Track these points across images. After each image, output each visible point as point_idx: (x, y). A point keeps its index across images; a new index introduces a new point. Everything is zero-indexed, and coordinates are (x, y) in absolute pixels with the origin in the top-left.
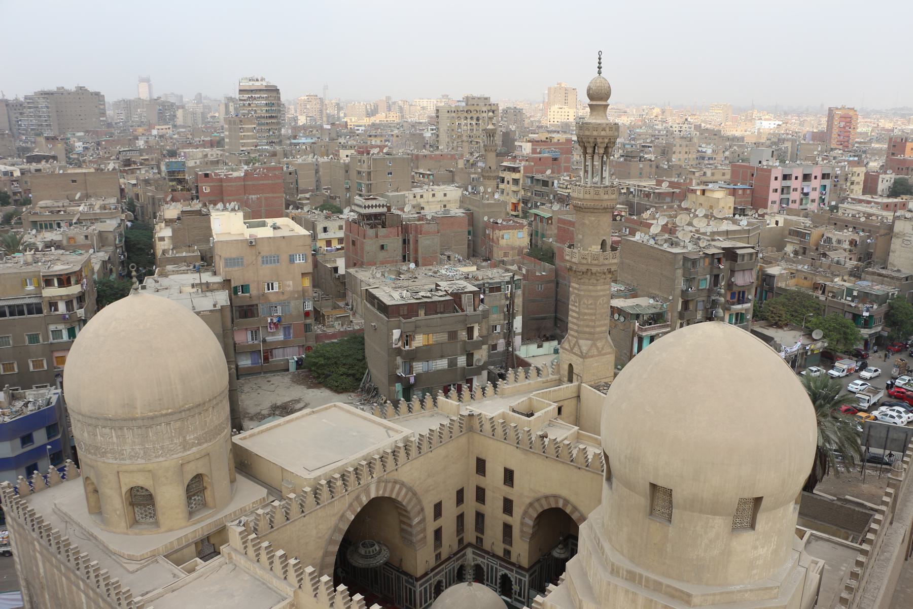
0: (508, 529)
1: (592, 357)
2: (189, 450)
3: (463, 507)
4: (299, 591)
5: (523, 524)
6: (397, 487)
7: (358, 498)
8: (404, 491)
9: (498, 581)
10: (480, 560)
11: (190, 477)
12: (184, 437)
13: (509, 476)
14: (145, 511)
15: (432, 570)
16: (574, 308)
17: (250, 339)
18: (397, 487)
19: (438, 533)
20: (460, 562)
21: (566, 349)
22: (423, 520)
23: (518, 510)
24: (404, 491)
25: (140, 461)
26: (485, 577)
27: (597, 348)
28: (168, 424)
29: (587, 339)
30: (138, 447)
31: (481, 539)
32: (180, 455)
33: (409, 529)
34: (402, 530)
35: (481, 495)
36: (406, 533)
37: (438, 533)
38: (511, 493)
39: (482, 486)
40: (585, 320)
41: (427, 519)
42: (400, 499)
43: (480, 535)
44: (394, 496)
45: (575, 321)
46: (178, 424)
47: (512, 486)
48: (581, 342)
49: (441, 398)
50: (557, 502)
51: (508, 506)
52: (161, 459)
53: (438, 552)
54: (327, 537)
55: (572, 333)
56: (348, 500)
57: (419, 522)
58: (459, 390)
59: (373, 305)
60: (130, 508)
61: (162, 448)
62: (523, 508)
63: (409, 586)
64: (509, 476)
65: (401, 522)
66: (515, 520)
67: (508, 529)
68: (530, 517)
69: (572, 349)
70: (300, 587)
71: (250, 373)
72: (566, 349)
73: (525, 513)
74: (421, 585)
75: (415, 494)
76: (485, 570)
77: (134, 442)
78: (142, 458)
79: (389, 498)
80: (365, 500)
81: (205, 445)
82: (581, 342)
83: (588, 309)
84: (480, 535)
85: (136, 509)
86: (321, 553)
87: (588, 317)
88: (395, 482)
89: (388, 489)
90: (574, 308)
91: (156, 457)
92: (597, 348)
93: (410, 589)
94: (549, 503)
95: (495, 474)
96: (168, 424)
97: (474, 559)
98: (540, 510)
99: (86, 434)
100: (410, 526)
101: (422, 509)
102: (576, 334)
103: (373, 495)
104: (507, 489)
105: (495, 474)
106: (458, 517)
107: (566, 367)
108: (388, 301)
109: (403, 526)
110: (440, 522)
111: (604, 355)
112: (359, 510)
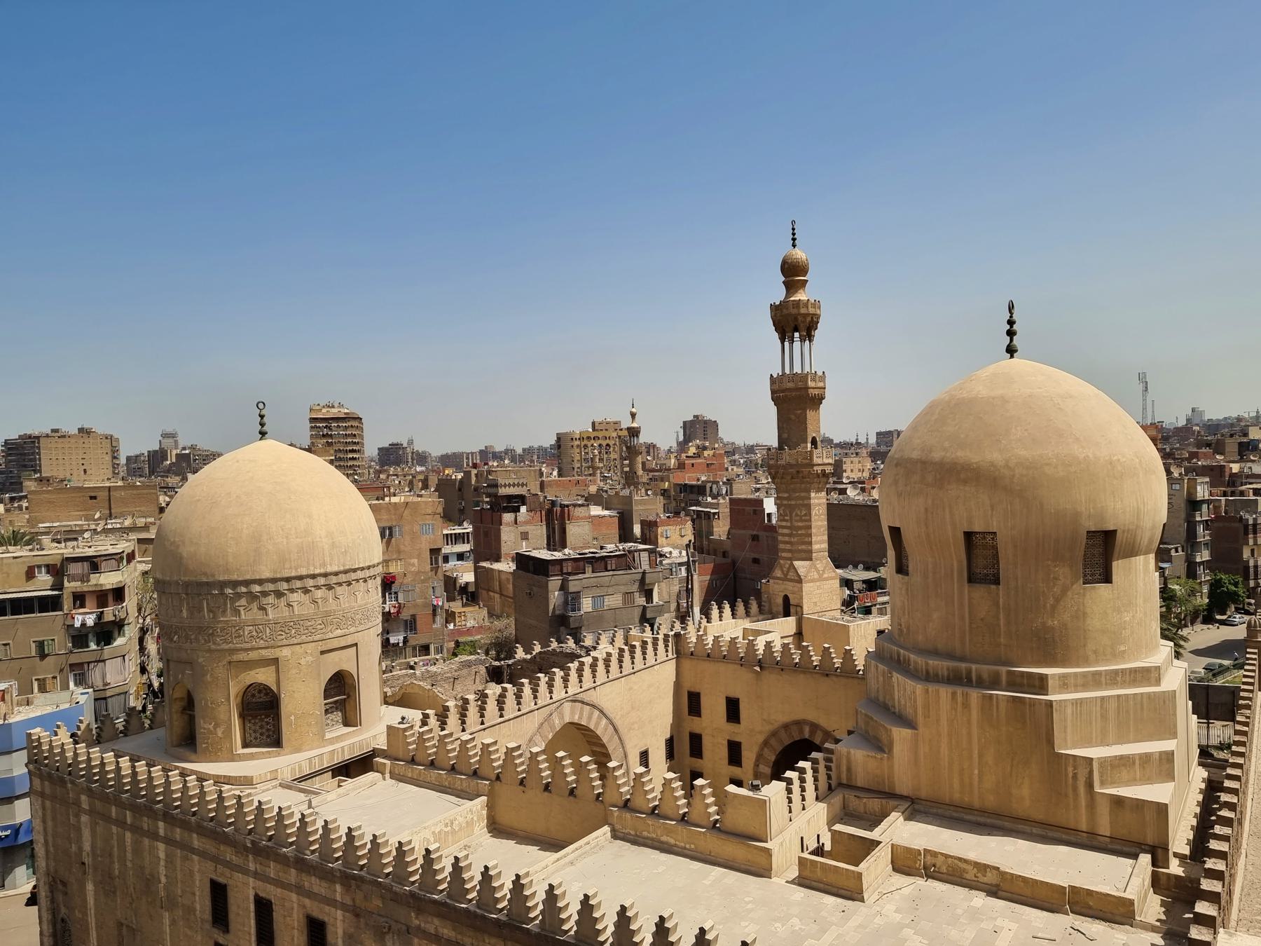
1: (813, 581)
13: (733, 710)
27: (818, 571)
38: (739, 732)
39: (697, 731)
40: (801, 535)
45: (787, 539)
47: (738, 722)
48: (796, 563)
50: (801, 731)
55: (784, 555)
56: (537, 717)
62: (756, 749)
64: (733, 710)
69: (786, 575)
73: (759, 758)
82: (796, 563)
92: (818, 571)
95: (713, 708)
102: (789, 555)
103: (567, 720)
104: (732, 727)
105: (713, 708)
107: (780, 601)
111: (827, 579)
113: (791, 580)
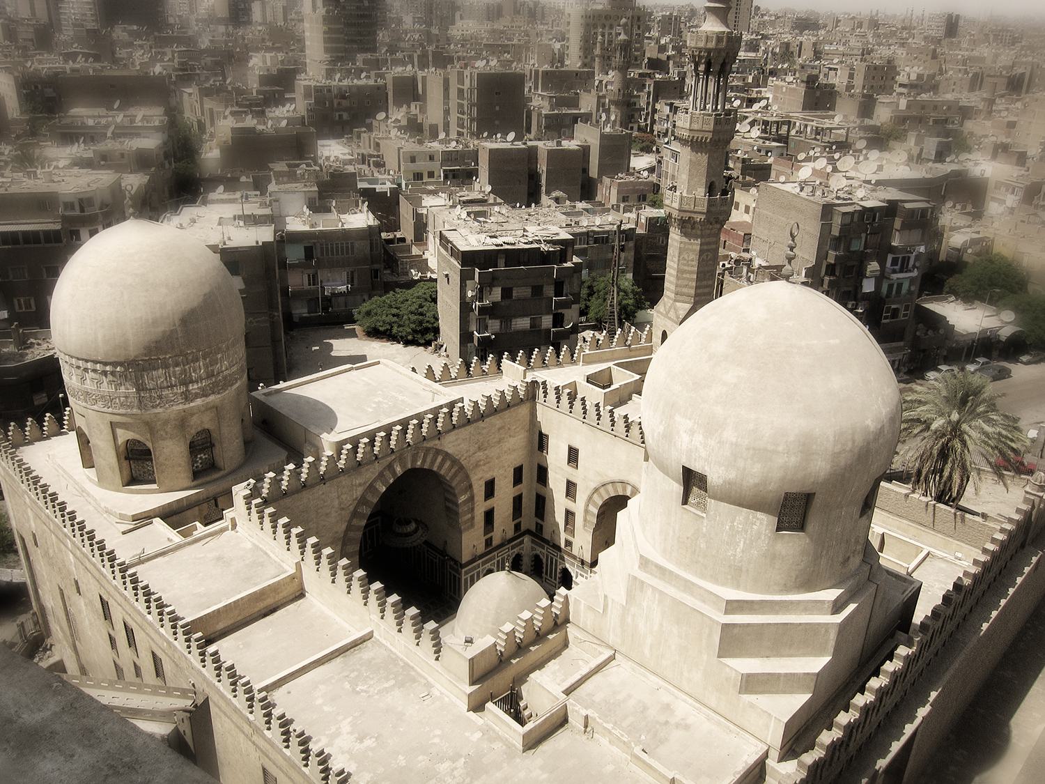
0: (569, 514)
3: (523, 488)
4: (302, 563)
5: (586, 511)
6: (439, 459)
7: (390, 467)
8: (448, 464)
9: (558, 575)
10: (539, 550)
13: (573, 455)
15: (481, 556)
16: (672, 264)
17: (306, 282)
18: (439, 459)
19: (489, 515)
20: (516, 550)
21: (661, 314)
22: (472, 498)
23: (582, 496)
24: (448, 464)
26: (544, 570)
29: (683, 302)
31: (542, 526)
32: (181, 407)
33: (454, 507)
34: (448, 509)
35: (542, 474)
36: (451, 512)
37: (489, 515)
38: (577, 476)
41: (476, 499)
42: (442, 472)
43: (540, 521)
44: (435, 469)
48: (678, 304)
49: (506, 363)
51: (571, 488)
53: (489, 536)
54: (352, 508)
57: (465, 502)
58: (529, 356)
59: (446, 249)
60: (125, 464)
61: (160, 397)
62: (588, 492)
63: (453, 572)
64: (573, 455)
65: (446, 499)
66: (578, 507)
67: (569, 514)
68: (595, 504)
70: (303, 560)
71: (306, 324)
72: (661, 314)
74: (466, 573)
75: (462, 468)
76: (544, 561)
79: (430, 471)
80: (399, 470)
81: (212, 398)
83: (688, 265)
84: (540, 521)
86: (344, 526)
87: (688, 276)
88: (438, 452)
89: (429, 460)
90: (672, 264)
91: (153, 407)
93: (455, 576)
94: (616, 490)
97: (533, 549)
98: (606, 497)
99: (74, 377)
100: (457, 505)
101: (470, 486)
103: (409, 466)
104: (569, 469)
106: (514, 498)
108: (463, 247)
109: (447, 504)
110: (490, 503)
112: (391, 481)
113: (670, 318)
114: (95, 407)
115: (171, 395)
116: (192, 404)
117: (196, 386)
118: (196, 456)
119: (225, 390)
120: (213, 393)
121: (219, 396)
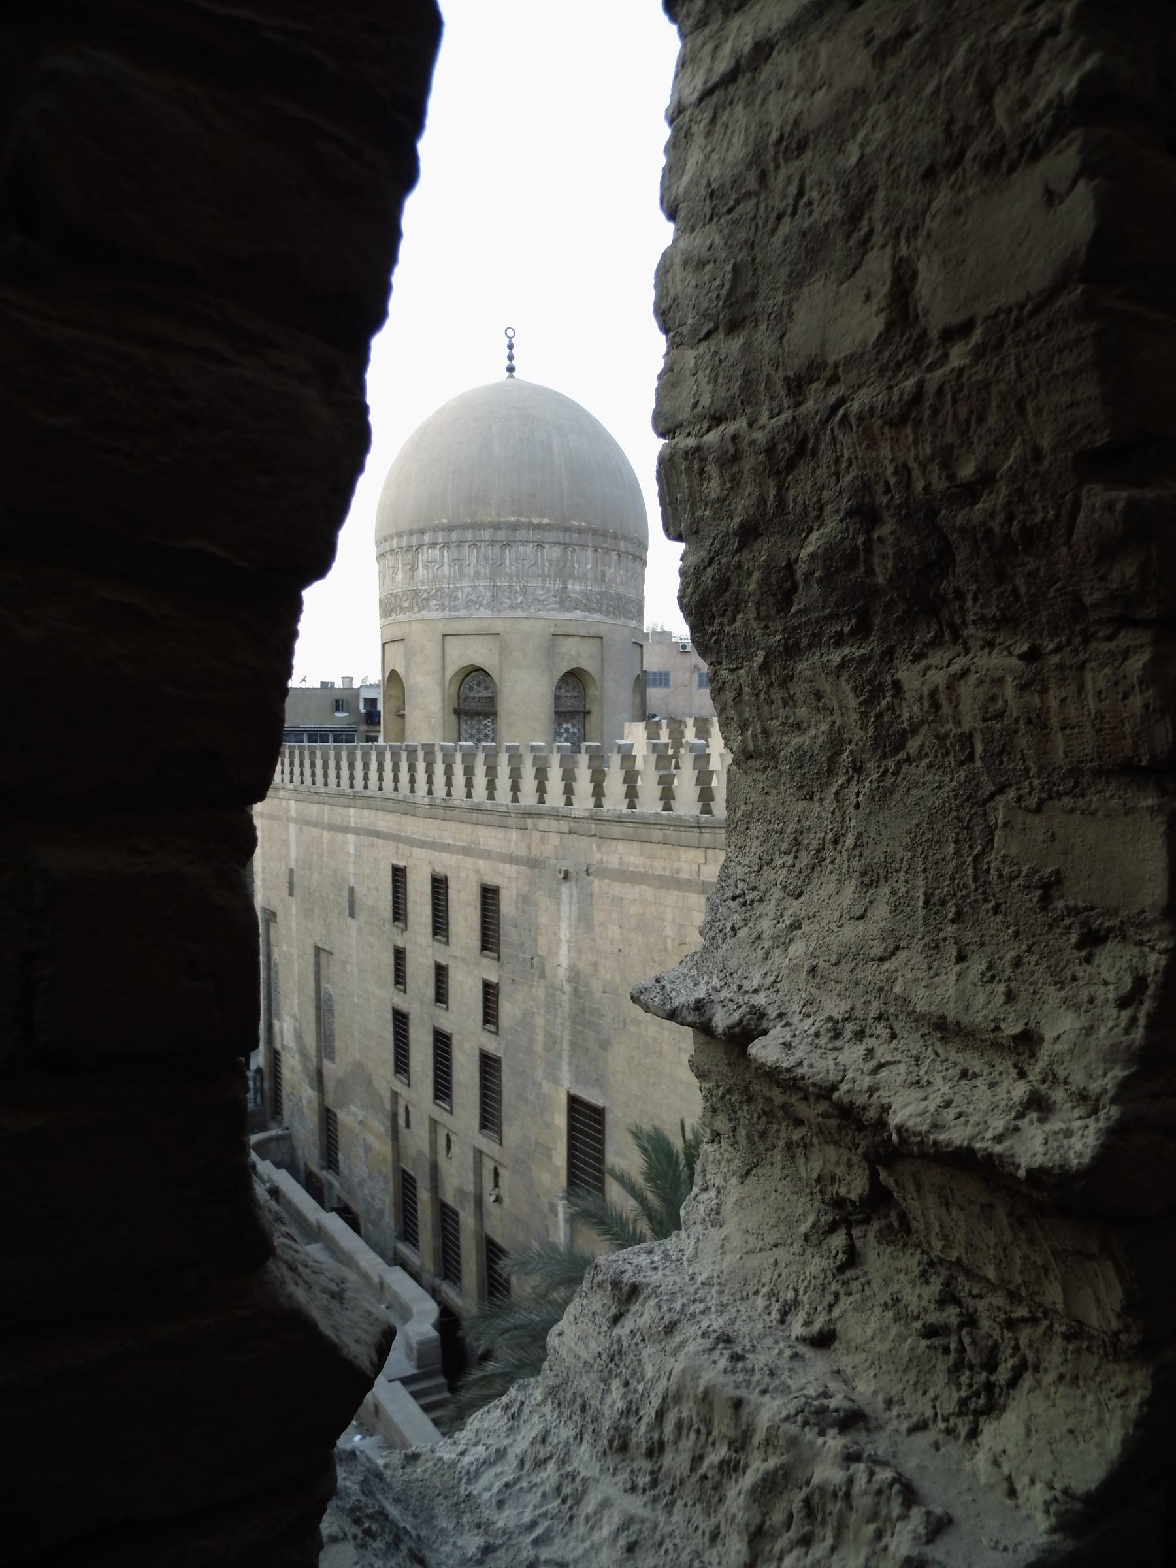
2: (569, 610)
11: (565, 668)
12: (565, 582)
14: (479, 731)
25: (484, 612)
28: (540, 545)
30: (482, 583)
32: (553, 614)
46: (556, 552)
52: (519, 613)
60: (454, 718)
61: (524, 592)
77: (477, 573)
78: (489, 606)
81: (597, 617)
85: (464, 727)
91: (511, 607)
96: (540, 545)
114: (425, 614)
115: (541, 592)
116: (568, 616)
117: (577, 588)
118: (560, 725)
119: (618, 618)
120: (600, 611)
121: (606, 619)
